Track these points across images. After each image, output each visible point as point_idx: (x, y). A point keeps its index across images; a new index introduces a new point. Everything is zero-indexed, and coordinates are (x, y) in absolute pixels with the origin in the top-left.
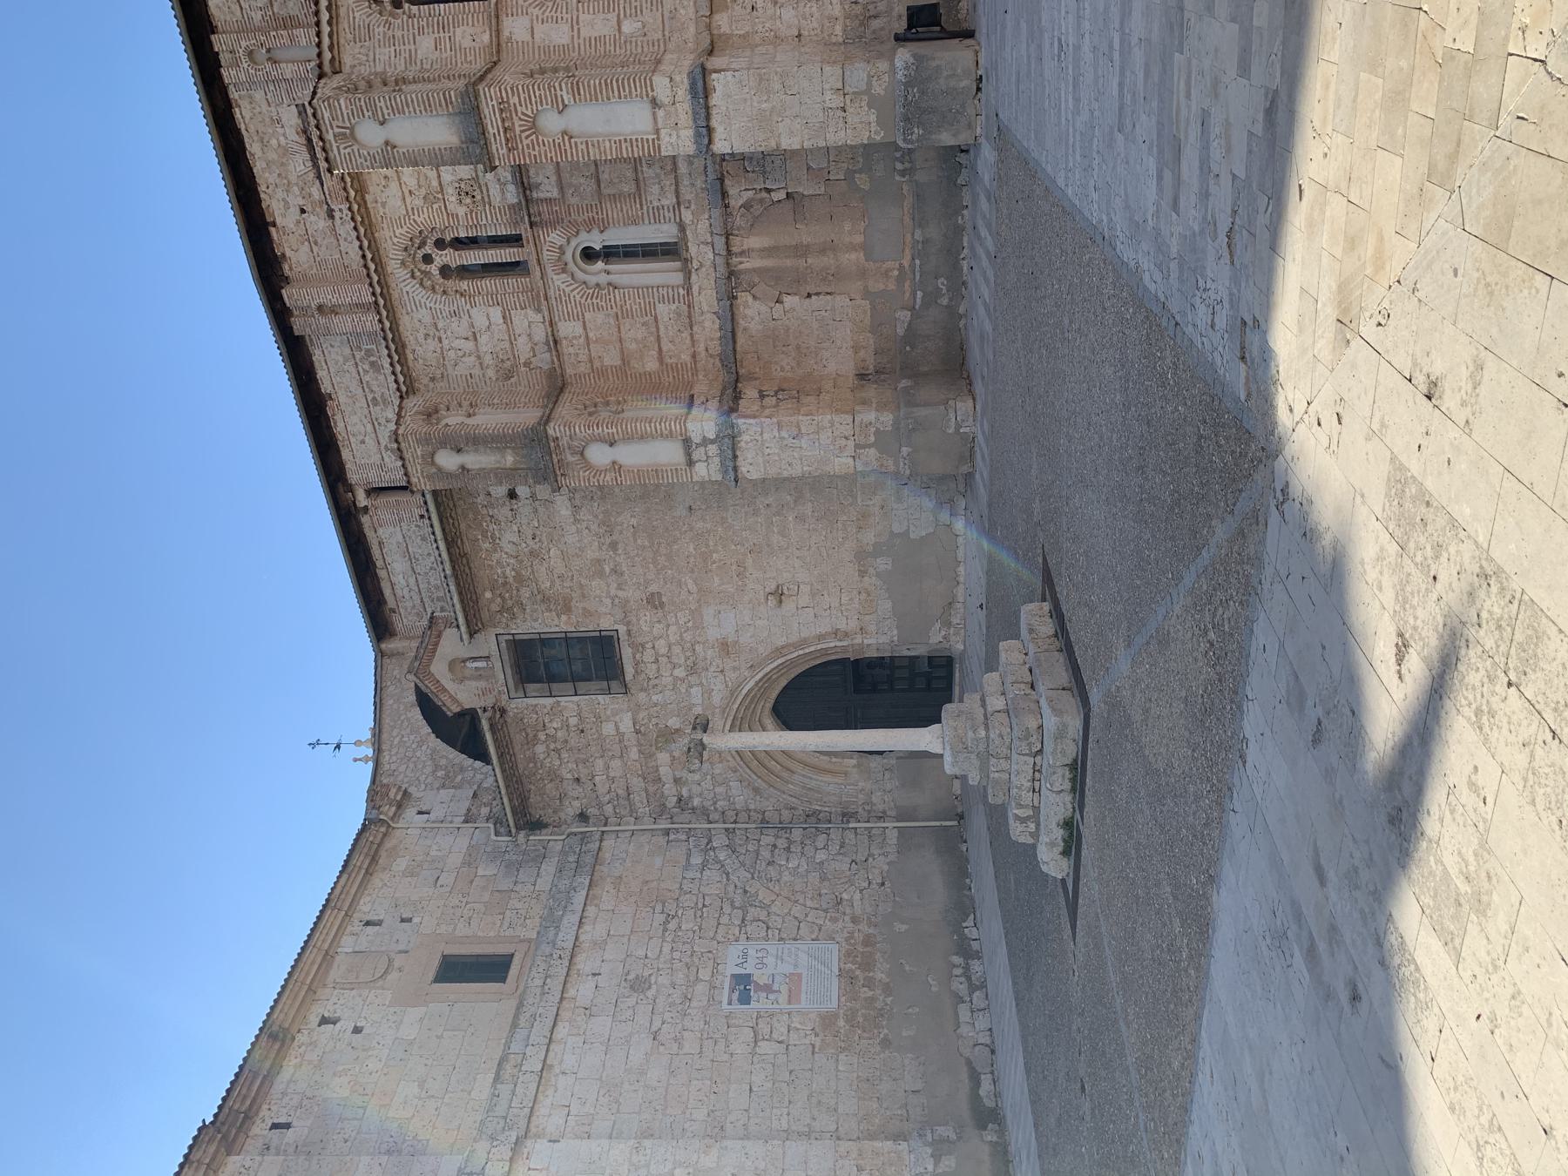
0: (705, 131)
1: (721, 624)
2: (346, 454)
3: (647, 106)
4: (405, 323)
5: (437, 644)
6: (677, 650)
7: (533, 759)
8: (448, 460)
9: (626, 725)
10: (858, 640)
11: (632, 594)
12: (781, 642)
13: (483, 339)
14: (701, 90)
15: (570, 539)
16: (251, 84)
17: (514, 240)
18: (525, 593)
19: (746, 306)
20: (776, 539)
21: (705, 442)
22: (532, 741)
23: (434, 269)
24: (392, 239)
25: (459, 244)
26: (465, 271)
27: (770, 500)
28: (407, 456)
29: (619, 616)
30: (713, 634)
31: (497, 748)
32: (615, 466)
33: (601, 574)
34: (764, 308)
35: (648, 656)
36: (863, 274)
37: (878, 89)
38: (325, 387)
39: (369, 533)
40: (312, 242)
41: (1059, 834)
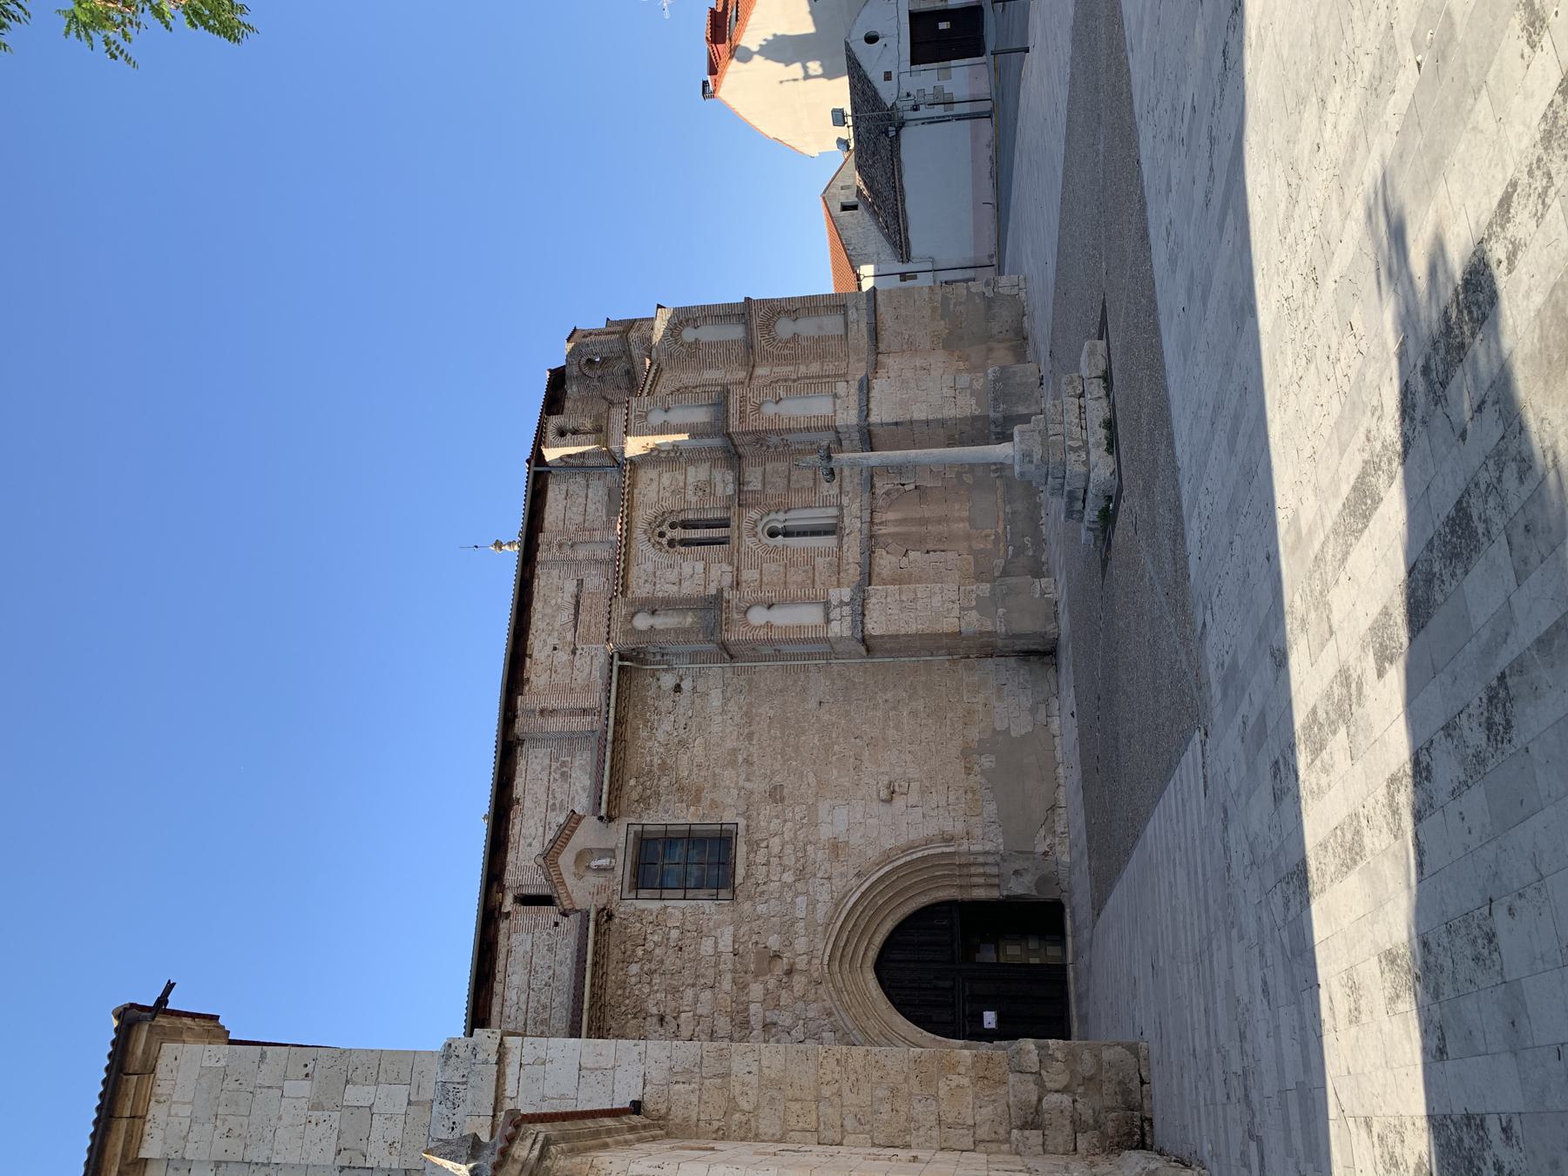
0: (865, 410)
1: (835, 821)
2: (511, 856)
3: (831, 400)
4: (634, 571)
5: (573, 832)
6: (789, 849)
7: (622, 985)
8: (642, 622)
9: (726, 944)
10: (964, 848)
11: (759, 786)
12: (889, 843)
13: (685, 584)
14: (865, 388)
15: (715, 729)
16: (555, 562)
17: (724, 523)
18: (665, 782)
19: (881, 557)
20: (891, 732)
21: (842, 604)
22: (626, 961)
23: (664, 541)
24: (642, 516)
25: (686, 525)
26: (686, 543)
27: (889, 696)
28: (614, 615)
29: (742, 809)
30: (826, 832)
31: (595, 953)
32: (769, 625)
33: (733, 763)
34: (893, 559)
35: (760, 857)
36: (968, 537)
37: (977, 385)
38: (518, 792)
39: (502, 940)
40: (552, 670)
41: (1102, 433)
